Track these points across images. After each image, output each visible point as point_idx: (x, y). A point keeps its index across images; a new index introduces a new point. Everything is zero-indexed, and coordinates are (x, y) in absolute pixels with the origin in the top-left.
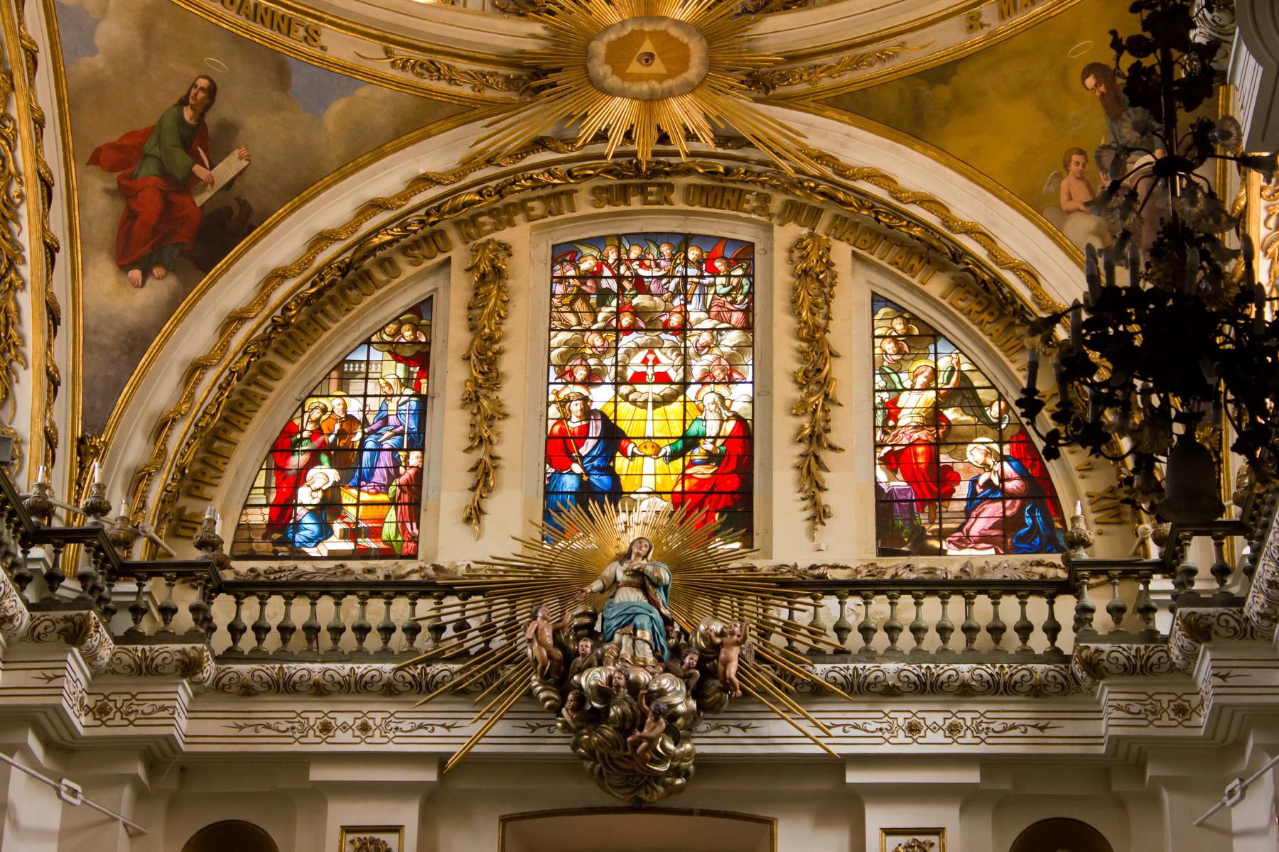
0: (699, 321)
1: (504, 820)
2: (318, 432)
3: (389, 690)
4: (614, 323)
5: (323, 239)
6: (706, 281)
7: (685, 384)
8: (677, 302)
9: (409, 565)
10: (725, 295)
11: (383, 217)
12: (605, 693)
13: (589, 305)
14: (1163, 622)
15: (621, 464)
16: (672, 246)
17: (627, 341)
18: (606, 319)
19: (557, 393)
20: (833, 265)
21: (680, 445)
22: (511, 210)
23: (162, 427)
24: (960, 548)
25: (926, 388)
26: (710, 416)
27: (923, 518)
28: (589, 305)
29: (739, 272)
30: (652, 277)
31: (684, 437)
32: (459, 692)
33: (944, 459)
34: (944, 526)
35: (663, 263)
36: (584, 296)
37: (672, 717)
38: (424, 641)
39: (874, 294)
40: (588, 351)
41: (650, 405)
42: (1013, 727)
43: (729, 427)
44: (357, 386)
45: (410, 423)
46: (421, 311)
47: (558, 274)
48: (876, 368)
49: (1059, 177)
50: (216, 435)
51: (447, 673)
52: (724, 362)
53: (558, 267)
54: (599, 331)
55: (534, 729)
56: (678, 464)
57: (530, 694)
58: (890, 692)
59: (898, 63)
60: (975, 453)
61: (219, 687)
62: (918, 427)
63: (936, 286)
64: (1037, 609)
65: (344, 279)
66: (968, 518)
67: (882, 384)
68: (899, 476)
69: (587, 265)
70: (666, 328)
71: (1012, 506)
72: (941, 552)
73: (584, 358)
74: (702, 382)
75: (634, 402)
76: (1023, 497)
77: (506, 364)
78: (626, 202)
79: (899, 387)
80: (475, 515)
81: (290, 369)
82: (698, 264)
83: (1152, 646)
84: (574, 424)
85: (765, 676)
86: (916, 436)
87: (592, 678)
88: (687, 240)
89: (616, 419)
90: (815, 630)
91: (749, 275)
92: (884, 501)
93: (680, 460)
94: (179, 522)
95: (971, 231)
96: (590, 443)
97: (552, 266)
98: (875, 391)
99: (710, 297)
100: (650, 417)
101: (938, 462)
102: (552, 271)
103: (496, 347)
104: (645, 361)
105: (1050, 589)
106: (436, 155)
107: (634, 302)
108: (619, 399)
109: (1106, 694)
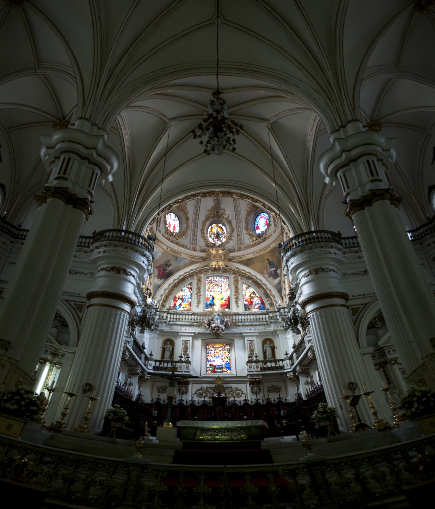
1: (202, 340)
2: (179, 297)
3: (188, 326)
5: (180, 276)
9: (190, 312)
11: (187, 274)
14: (278, 317)
22: (201, 273)
23: (162, 296)
27: (250, 307)
32: (197, 326)
37: (222, 329)
38: (193, 320)
43: (227, 297)
44: (183, 291)
45: (190, 296)
46: (191, 284)
50: (167, 296)
57: (205, 326)
58: (247, 326)
61: (168, 324)
63: (250, 281)
64: (264, 316)
65: (182, 280)
69: (210, 279)
76: (261, 304)
77: (201, 290)
80: (198, 306)
81: (176, 289)
84: (209, 297)
85: (233, 324)
90: (238, 320)
92: (245, 305)
94: (163, 306)
95: (254, 276)
105: (265, 314)
106: (194, 267)
109: (272, 325)
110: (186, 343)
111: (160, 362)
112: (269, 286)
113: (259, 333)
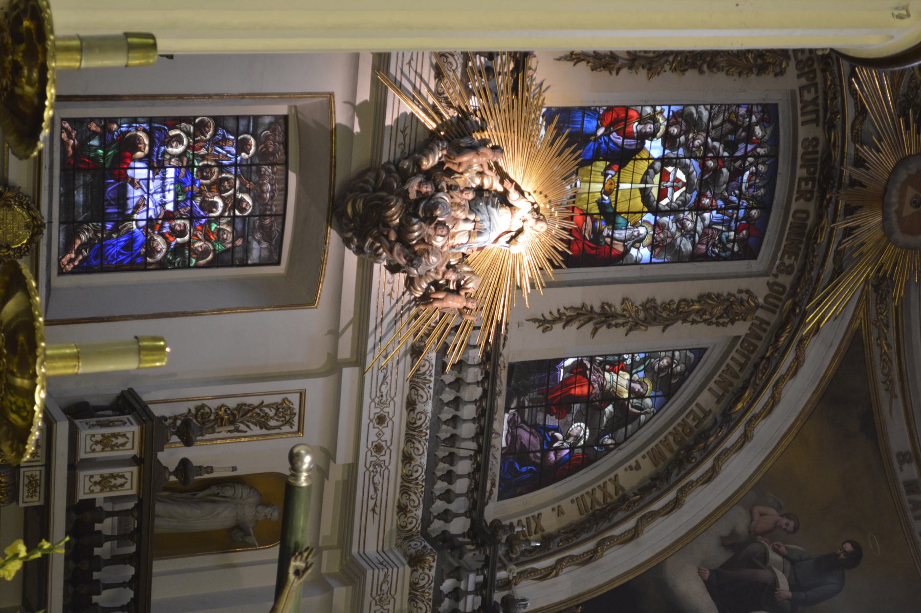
0: (703, 220)
4: (711, 155)
6: (733, 224)
7: (656, 211)
8: (720, 203)
10: (720, 239)
13: (727, 134)
15: (601, 165)
16: (763, 196)
17: (694, 165)
18: (714, 147)
19: (661, 112)
20: (733, 323)
21: (611, 210)
24: (509, 422)
25: (631, 390)
26: (629, 232)
27: (533, 395)
28: (727, 134)
29: (736, 249)
30: (742, 182)
31: (616, 214)
33: (577, 407)
34: (527, 410)
35: (751, 190)
36: (734, 131)
39: (705, 350)
40: (691, 136)
41: (643, 186)
42: (376, 489)
43: (619, 247)
47: (755, 109)
48: (651, 354)
49: (779, 508)
51: (454, 68)
52: (669, 240)
53: (760, 108)
54: (705, 144)
55: (403, 132)
56: (596, 210)
59: (883, 394)
60: (578, 428)
62: (602, 387)
66: (530, 426)
67: (638, 359)
68: (567, 375)
70: (701, 195)
71: (536, 457)
72: (507, 409)
73: (686, 133)
74: (656, 225)
75: (647, 173)
78: (801, 167)
79: (634, 371)
82: (747, 217)
83: (431, 604)
86: (596, 386)
88: (765, 205)
89: (636, 159)
91: (734, 257)
93: (597, 211)
96: (620, 141)
97: (761, 104)
98: (633, 354)
99: (720, 227)
100: (634, 186)
101: (574, 403)
102: (757, 105)
103: (705, 67)
104: (677, 180)
107: (725, 170)
108: (651, 161)
112: (659, 535)
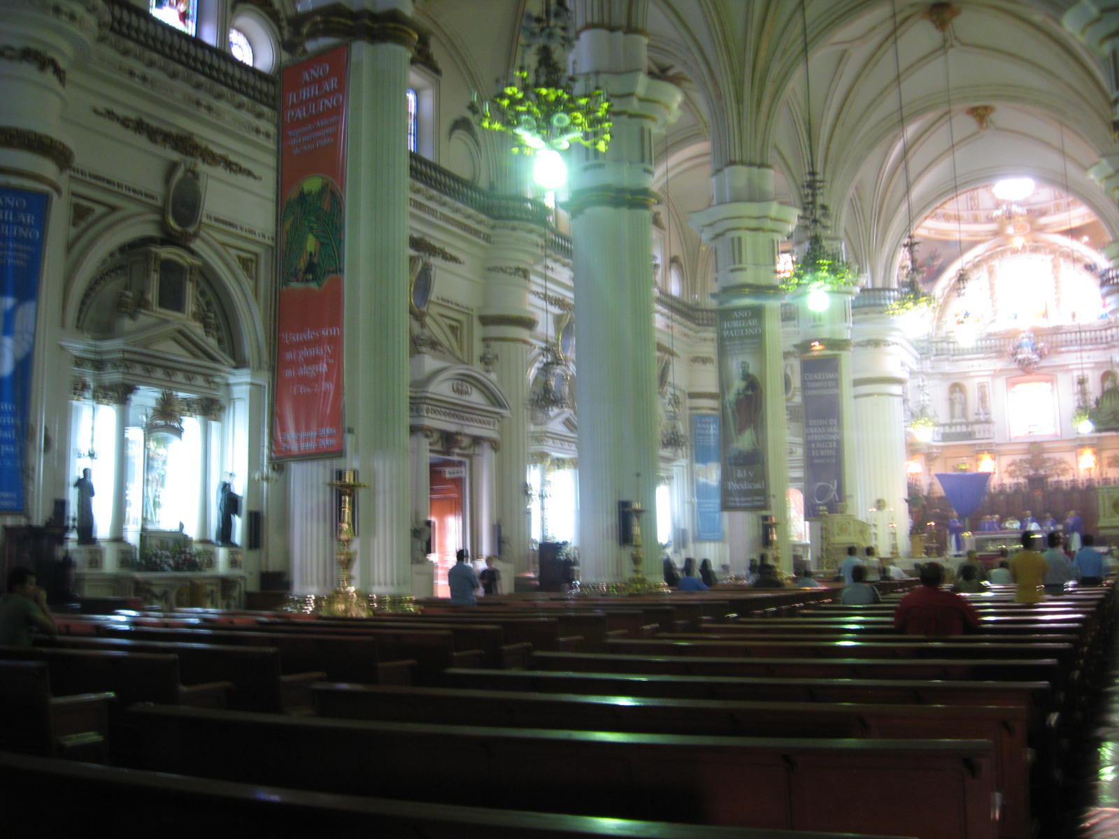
1: (1007, 379)
12: (1024, 360)
87: (1020, 357)
110: (982, 388)
111: (950, 425)
113: (1096, 363)
